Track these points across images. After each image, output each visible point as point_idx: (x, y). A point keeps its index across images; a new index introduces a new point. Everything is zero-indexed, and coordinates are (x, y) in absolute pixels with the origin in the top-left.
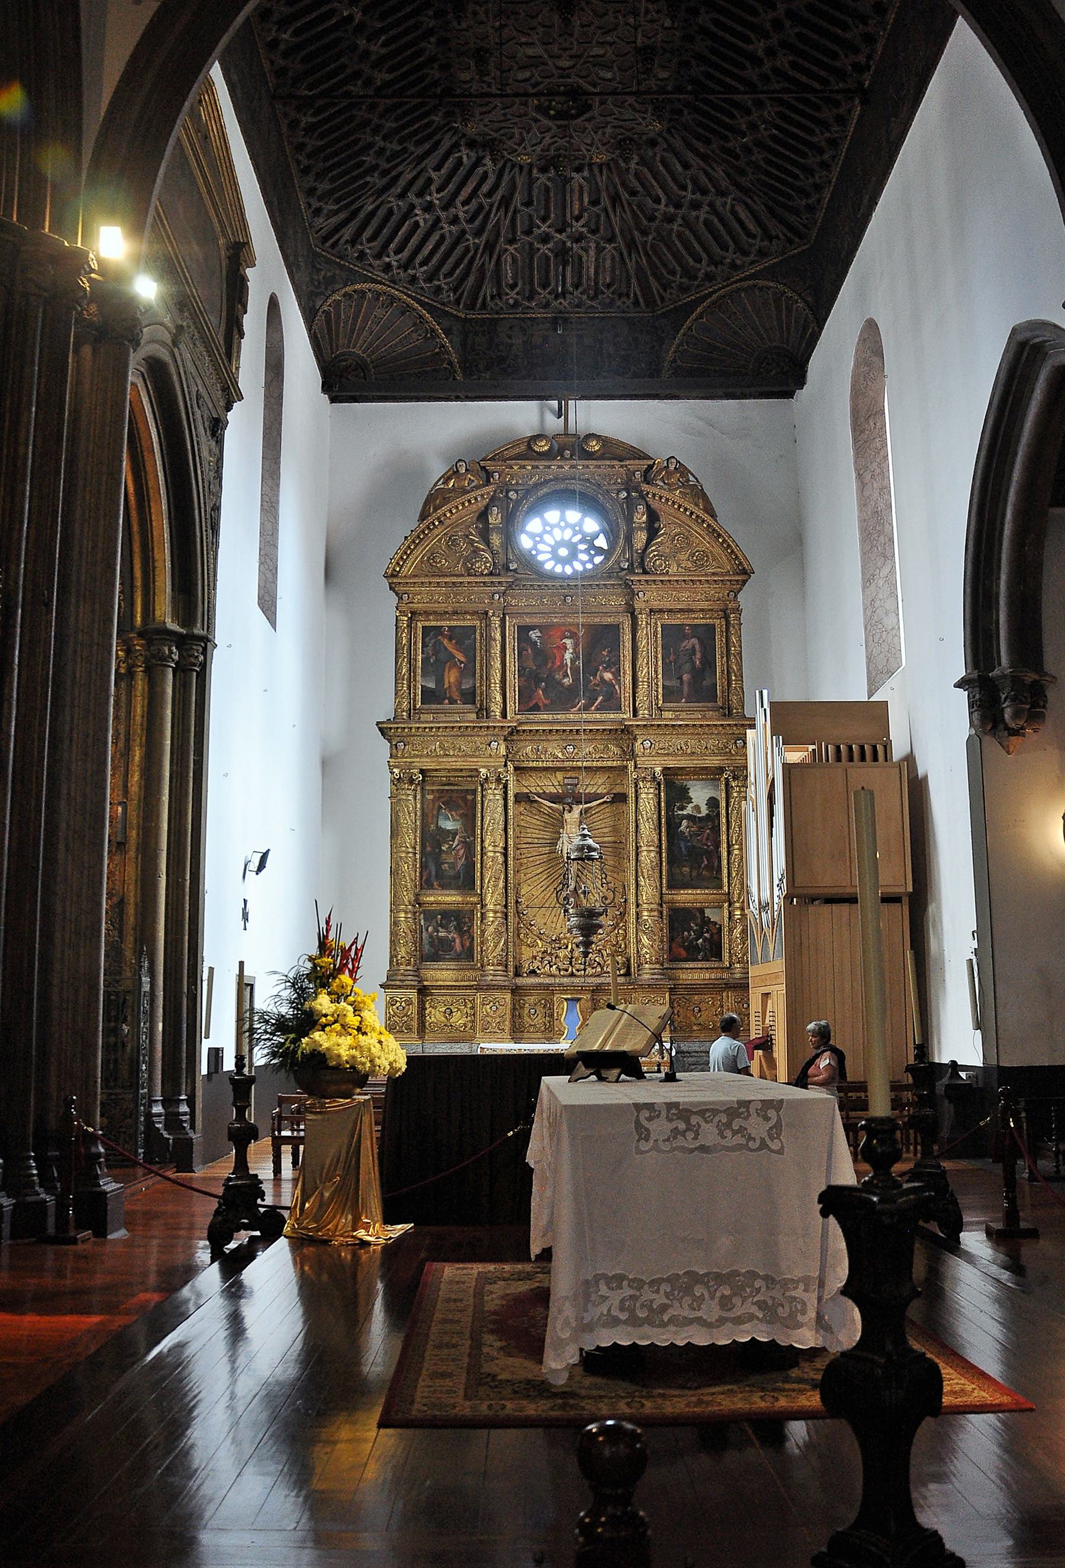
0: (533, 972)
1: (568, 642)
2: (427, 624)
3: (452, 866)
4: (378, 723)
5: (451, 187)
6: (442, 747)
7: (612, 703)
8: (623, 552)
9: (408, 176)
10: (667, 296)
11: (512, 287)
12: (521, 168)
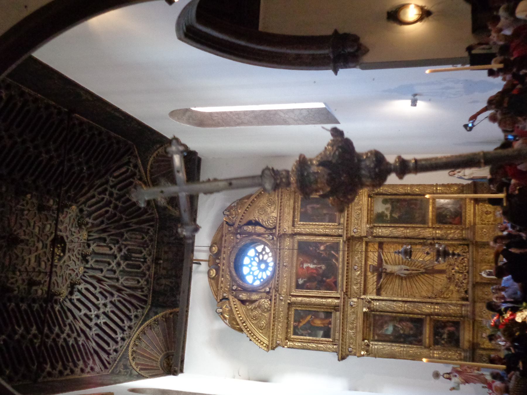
0: (466, 292)
1: (305, 265)
2: (292, 332)
3: (411, 329)
4: (339, 360)
5: (90, 305)
6: (352, 329)
7: (335, 247)
8: (264, 237)
9: (82, 325)
10: (150, 212)
11: (139, 282)
12: (85, 272)
